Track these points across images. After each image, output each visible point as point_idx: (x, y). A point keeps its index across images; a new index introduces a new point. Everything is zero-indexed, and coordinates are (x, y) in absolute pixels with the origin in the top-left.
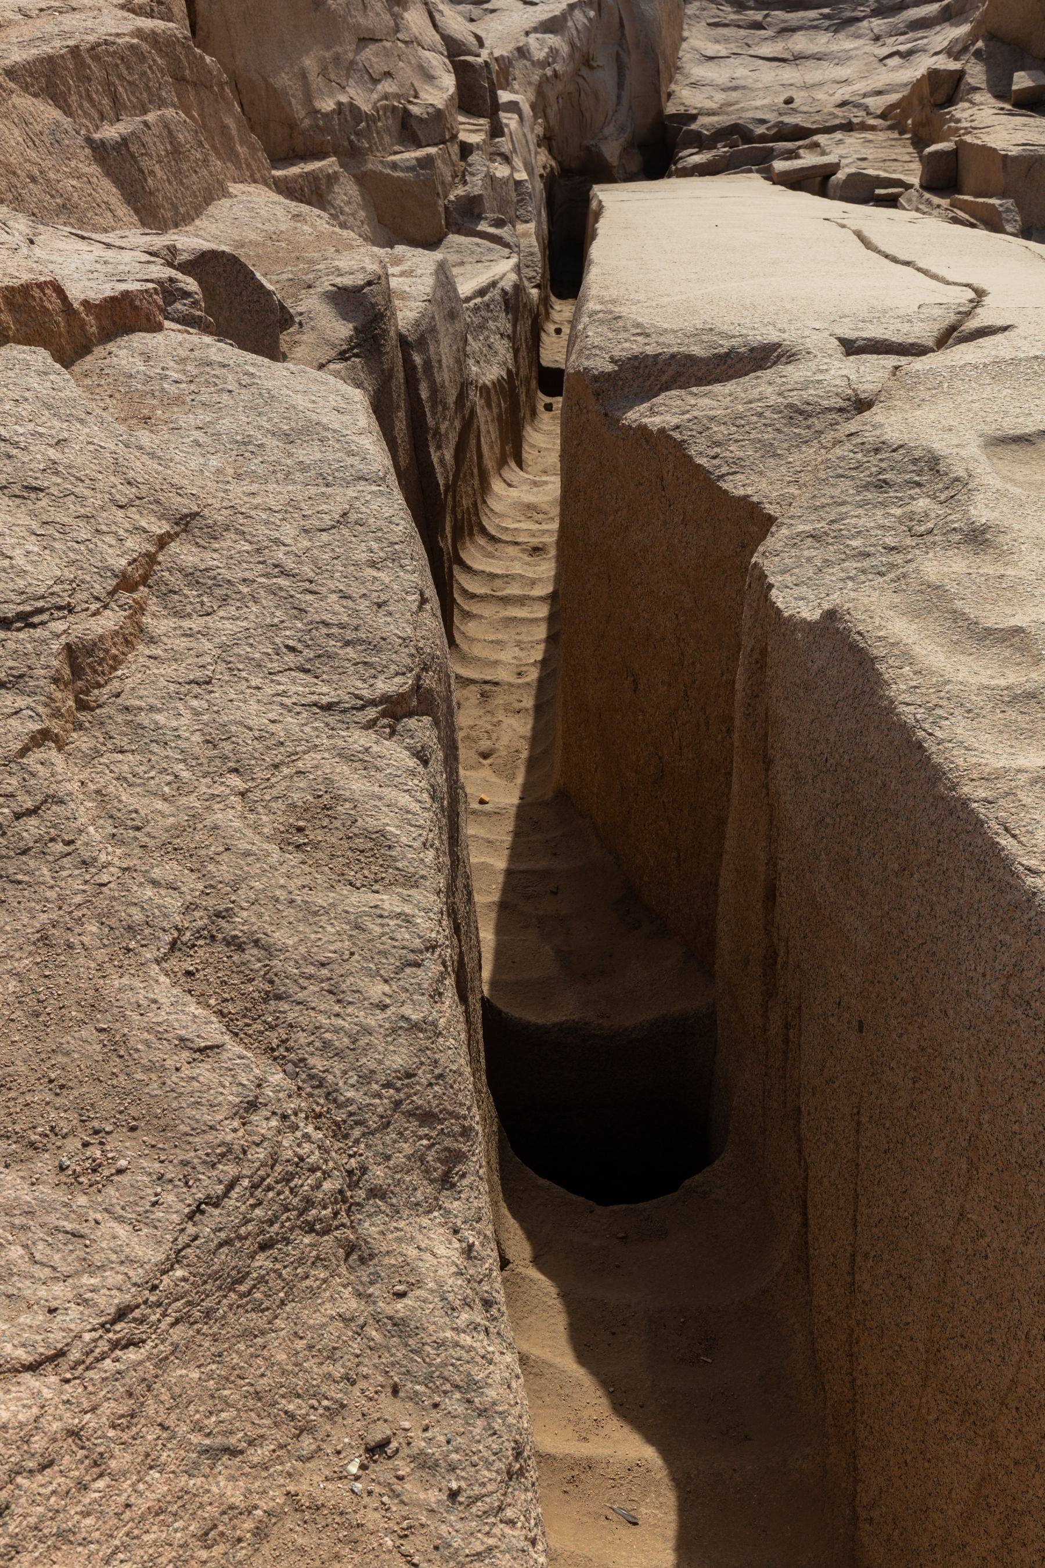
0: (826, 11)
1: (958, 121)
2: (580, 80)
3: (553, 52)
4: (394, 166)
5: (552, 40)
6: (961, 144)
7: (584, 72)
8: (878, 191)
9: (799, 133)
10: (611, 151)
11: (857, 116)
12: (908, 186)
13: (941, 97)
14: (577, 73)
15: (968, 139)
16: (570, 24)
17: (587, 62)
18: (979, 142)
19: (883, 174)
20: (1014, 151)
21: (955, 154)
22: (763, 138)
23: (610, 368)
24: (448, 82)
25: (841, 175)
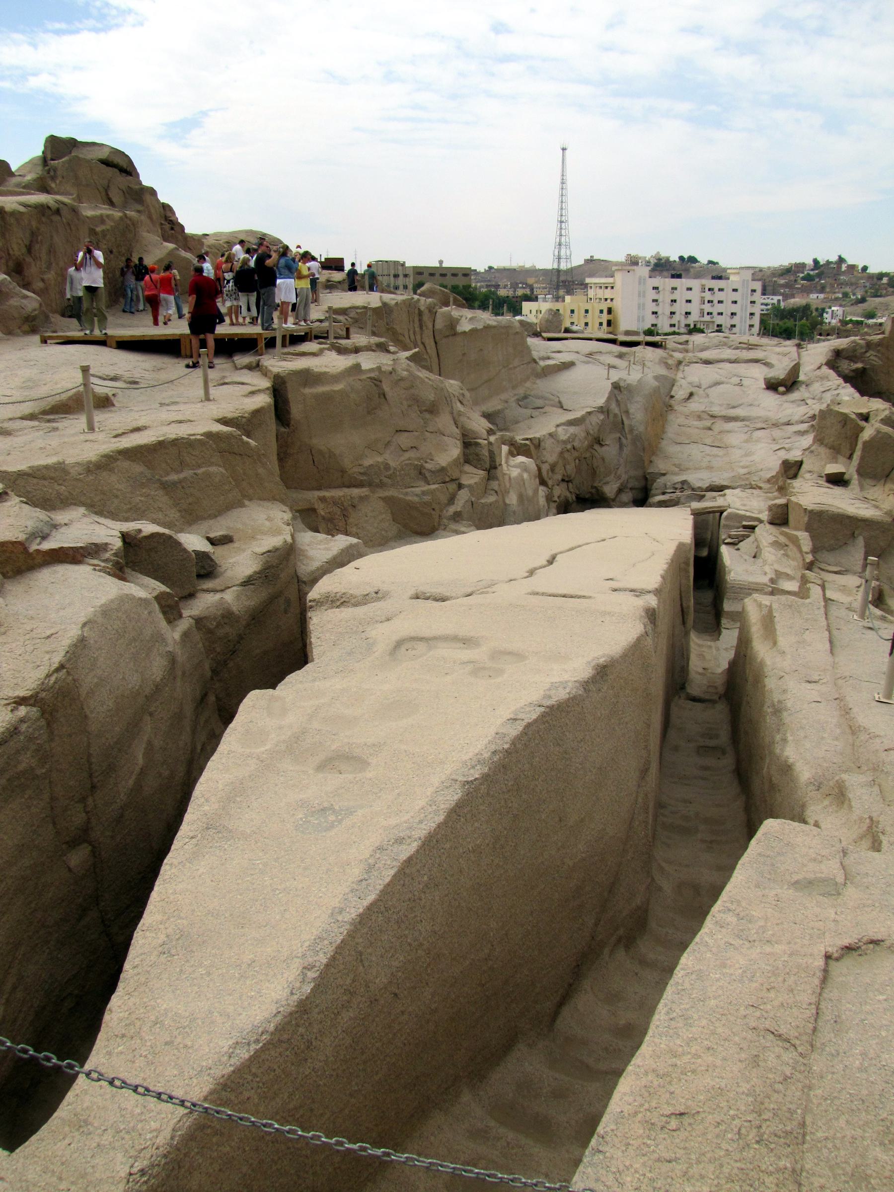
0: (747, 423)
1: (794, 488)
2: (594, 452)
3: (573, 437)
4: (407, 494)
5: (572, 430)
6: (789, 500)
7: (596, 447)
8: (744, 523)
9: (720, 489)
10: (610, 490)
11: (754, 480)
12: (761, 521)
14: (591, 446)
15: (793, 498)
16: (587, 422)
17: (598, 441)
18: (796, 500)
19: (748, 514)
21: (786, 505)
22: (700, 489)
24: (455, 451)
25: (725, 514)
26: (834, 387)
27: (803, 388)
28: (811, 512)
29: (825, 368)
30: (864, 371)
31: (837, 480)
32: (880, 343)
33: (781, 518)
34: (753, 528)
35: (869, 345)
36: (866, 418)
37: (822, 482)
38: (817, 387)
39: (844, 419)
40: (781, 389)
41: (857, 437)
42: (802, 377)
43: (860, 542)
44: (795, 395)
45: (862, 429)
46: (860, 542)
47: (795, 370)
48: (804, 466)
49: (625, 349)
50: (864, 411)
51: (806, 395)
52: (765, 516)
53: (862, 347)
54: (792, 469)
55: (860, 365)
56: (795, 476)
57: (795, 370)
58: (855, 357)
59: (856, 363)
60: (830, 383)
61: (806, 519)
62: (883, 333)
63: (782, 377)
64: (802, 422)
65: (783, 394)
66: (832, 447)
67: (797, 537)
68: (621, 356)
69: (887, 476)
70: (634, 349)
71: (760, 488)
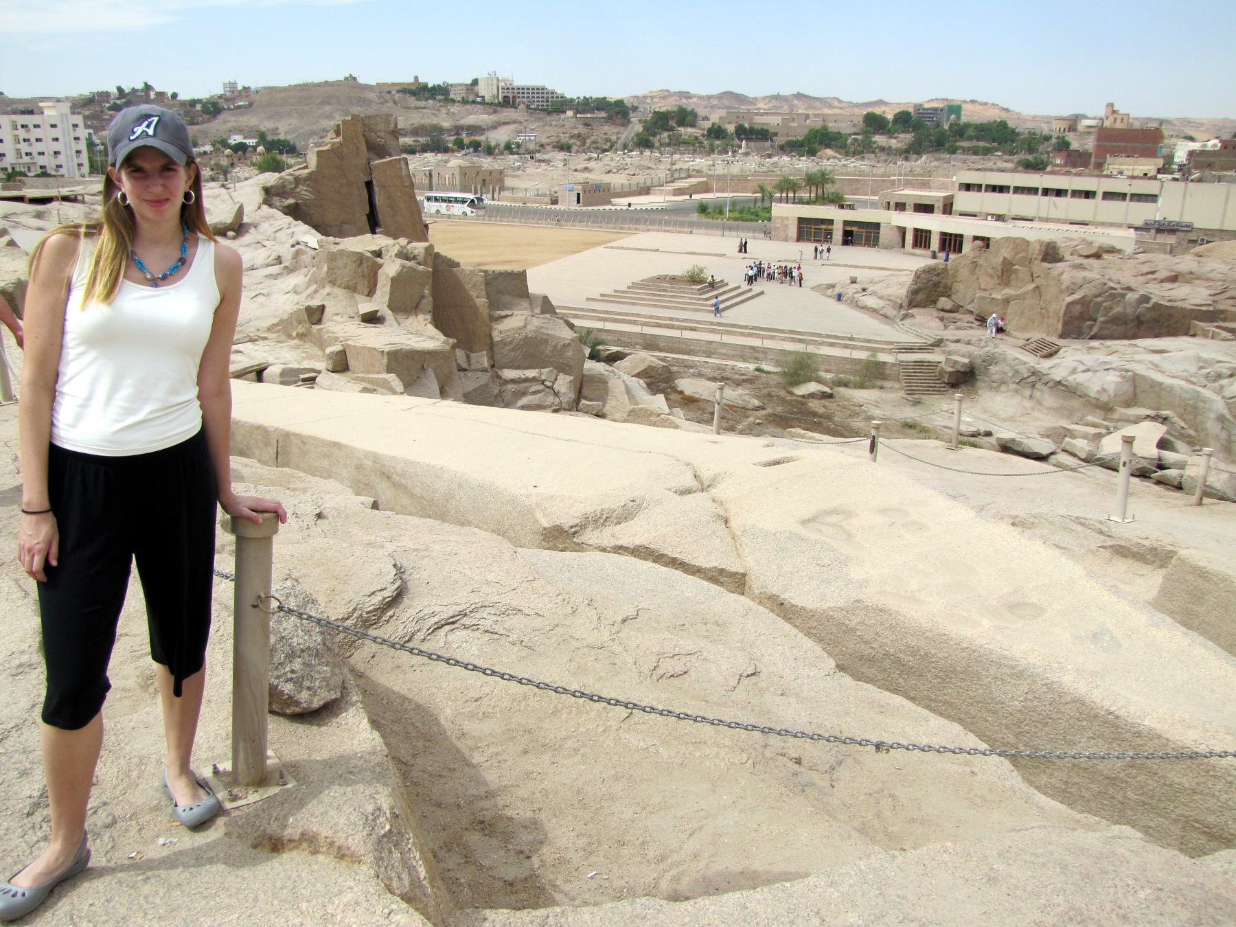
8: (302, 376)
12: (319, 372)
13: (315, 318)
20: (386, 349)
21: (343, 352)
23: (577, 521)
26: (286, 226)
27: (252, 230)
28: (388, 353)
29: (265, 207)
30: (297, 204)
31: (372, 319)
32: (310, 177)
33: (341, 365)
34: (313, 379)
35: (297, 180)
36: (378, 254)
37: (358, 321)
38: (265, 227)
39: (360, 258)
40: (231, 234)
41: (376, 274)
42: (246, 220)
43: (431, 373)
44: (247, 239)
45: (381, 266)
46: (431, 373)
47: (240, 212)
48: (327, 310)
49: (40, 208)
50: (376, 248)
51: (259, 238)
52: (321, 365)
53: (290, 183)
54: (316, 314)
55: (291, 201)
56: (319, 321)
57: (240, 212)
58: (285, 192)
59: (286, 198)
60: (279, 223)
61: (385, 360)
62: (306, 167)
63: (229, 221)
64: (268, 265)
65: (234, 238)
66: (347, 287)
67: (385, 380)
68: (39, 216)
69: (416, 307)
70: (49, 206)
71: (265, 338)
